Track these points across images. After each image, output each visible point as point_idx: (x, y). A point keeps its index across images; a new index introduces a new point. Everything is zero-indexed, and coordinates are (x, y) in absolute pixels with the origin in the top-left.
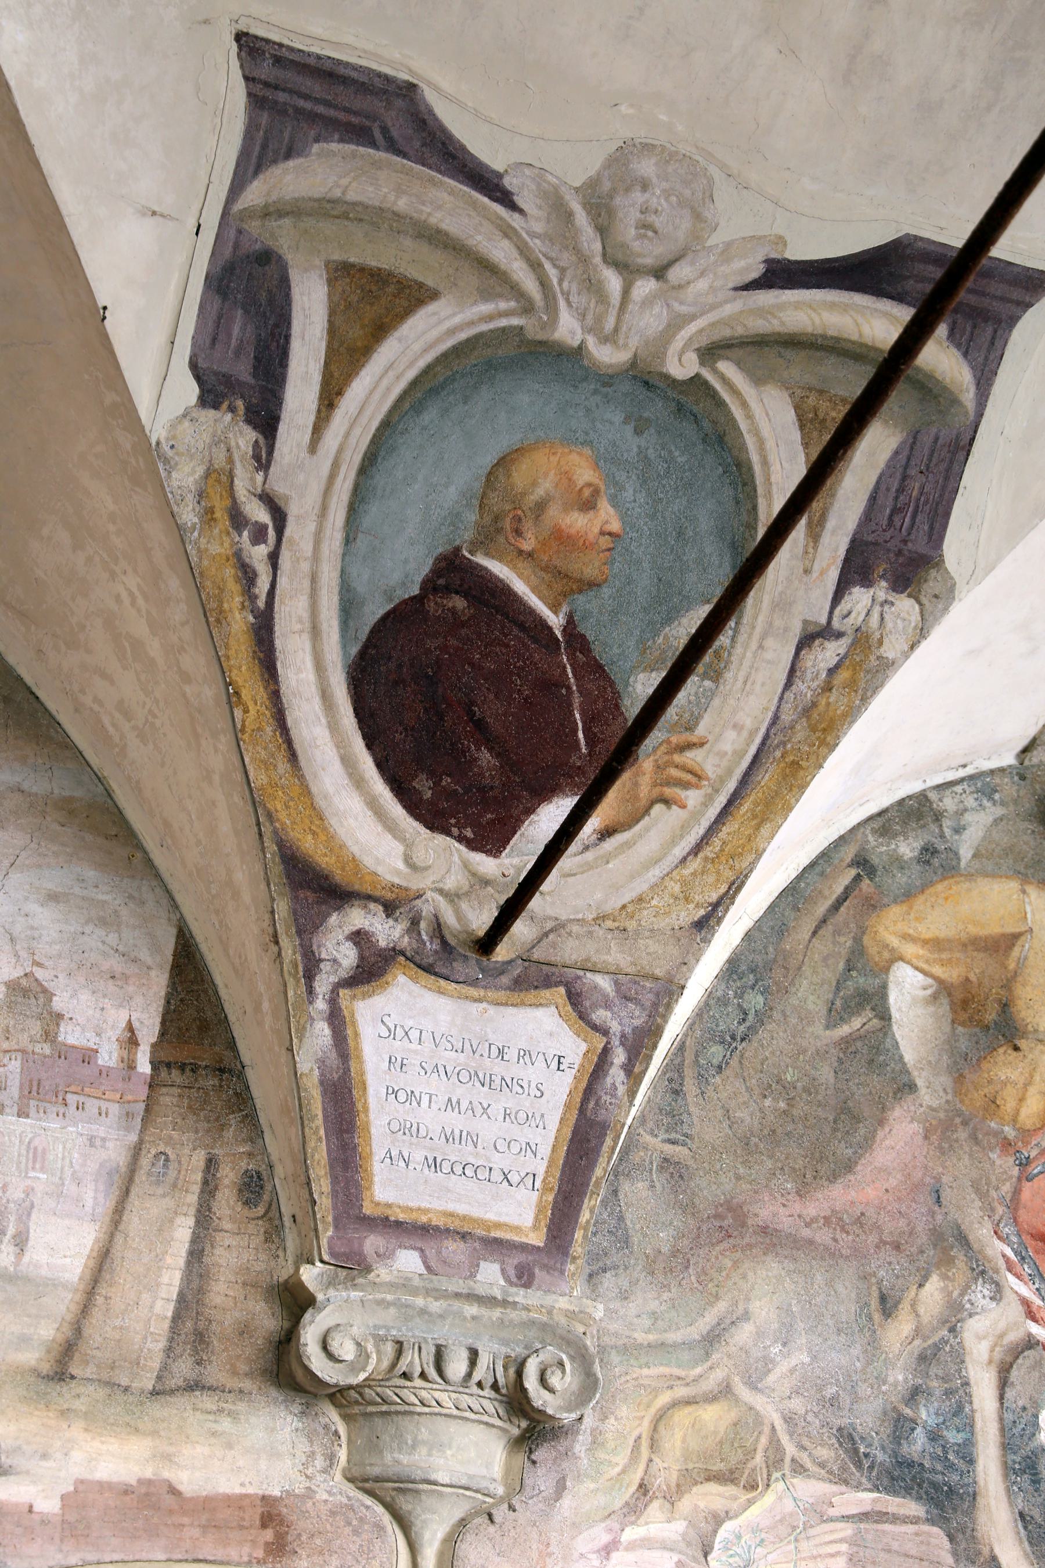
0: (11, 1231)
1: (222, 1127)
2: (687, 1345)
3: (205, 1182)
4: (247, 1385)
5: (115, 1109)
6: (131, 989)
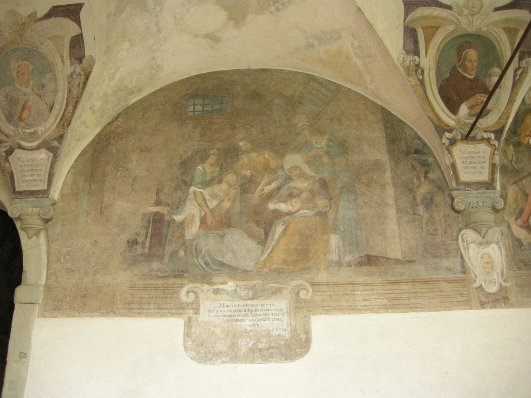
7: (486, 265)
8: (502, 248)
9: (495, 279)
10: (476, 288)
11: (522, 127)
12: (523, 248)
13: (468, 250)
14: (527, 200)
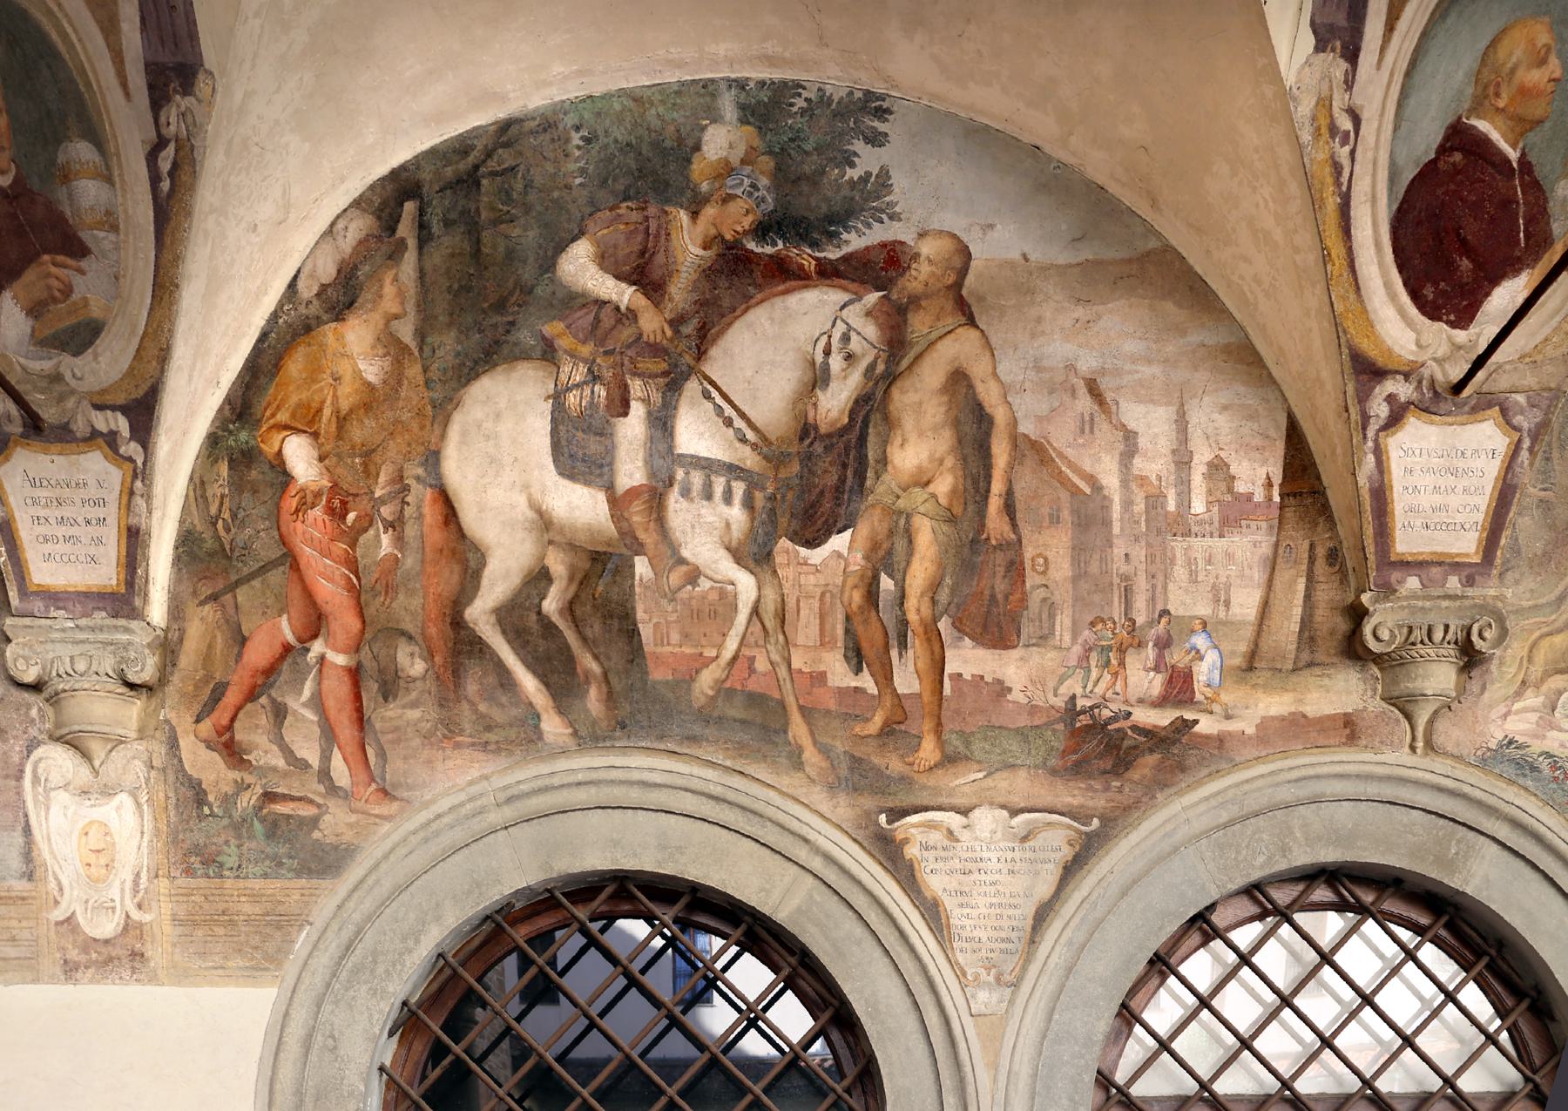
0: (1222, 599)
1: (1317, 525)
2: (1549, 604)
3: (1310, 557)
4: (1335, 660)
5: (1264, 525)
6: (1267, 454)
7: (92, 858)
8: (145, 807)
9: (112, 900)
10: (58, 924)
11: (271, 391)
12: (206, 810)
13: (48, 809)
14: (240, 655)
